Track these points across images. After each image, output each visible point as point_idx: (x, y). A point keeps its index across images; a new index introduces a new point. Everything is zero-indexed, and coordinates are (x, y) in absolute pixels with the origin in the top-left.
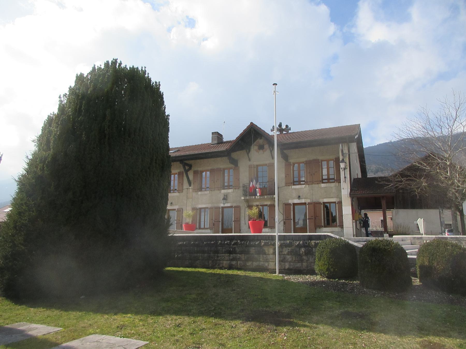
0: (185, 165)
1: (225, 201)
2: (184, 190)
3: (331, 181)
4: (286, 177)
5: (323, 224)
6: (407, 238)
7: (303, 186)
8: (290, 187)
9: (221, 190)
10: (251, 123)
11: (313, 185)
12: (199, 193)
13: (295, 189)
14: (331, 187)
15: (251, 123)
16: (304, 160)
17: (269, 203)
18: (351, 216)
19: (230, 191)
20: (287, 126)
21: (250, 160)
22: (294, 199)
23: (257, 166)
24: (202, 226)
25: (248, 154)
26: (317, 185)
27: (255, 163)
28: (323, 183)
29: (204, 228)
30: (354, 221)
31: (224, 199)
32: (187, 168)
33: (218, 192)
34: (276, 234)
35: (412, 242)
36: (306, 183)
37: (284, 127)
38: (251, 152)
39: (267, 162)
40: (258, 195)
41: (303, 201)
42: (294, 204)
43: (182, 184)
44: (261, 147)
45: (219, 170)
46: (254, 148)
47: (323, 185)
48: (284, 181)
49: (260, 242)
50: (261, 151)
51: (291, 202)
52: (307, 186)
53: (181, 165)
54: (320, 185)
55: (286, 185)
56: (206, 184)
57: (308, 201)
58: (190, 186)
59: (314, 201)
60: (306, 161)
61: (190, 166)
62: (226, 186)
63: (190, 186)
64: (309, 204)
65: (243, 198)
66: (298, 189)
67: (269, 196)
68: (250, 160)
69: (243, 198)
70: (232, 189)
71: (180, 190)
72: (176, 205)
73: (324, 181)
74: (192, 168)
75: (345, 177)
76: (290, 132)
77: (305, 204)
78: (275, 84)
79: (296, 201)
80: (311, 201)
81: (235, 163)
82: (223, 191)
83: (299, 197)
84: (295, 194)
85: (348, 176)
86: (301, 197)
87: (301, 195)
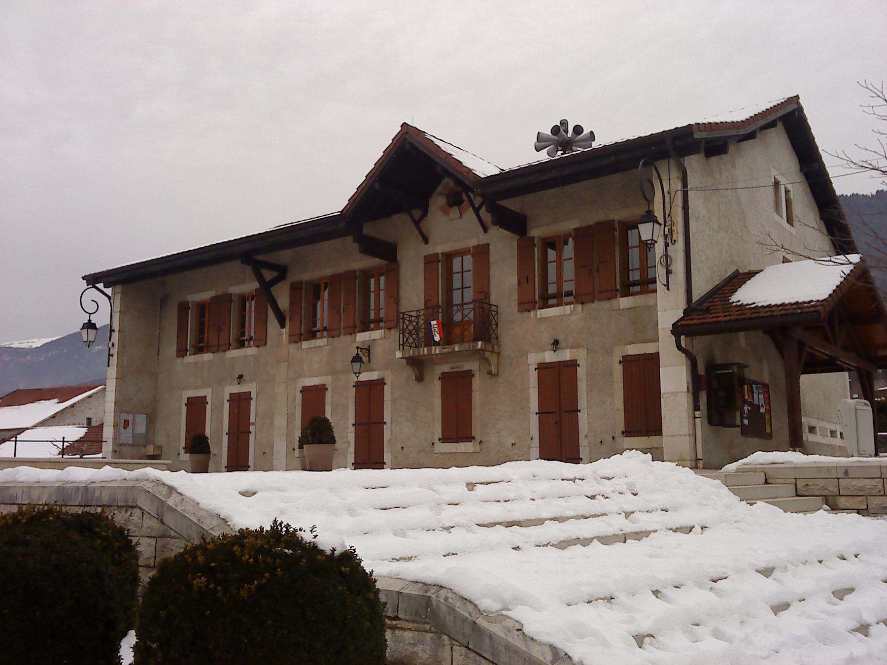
0: (257, 268)
1: (357, 366)
7: (568, 309)
8: (532, 313)
9: (355, 333)
11: (596, 305)
12: (305, 345)
13: (542, 319)
15: (404, 125)
16: (571, 225)
19: (377, 334)
21: (426, 241)
22: (543, 350)
23: (449, 257)
25: (417, 223)
26: (606, 304)
27: (440, 248)
30: (697, 413)
31: (357, 359)
32: (269, 275)
33: (348, 338)
36: (581, 297)
38: (430, 216)
39: (472, 243)
43: (265, 323)
44: (455, 201)
45: (350, 275)
47: (625, 302)
50: (455, 212)
52: (579, 307)
53: (248, 270)
60: (576, 230)
61: (282, 272)
65: (399, 354)
67: (466, 346)
68: (426, 241)
69: (399, 354)
72: (251, 381)
74: (288, 275)
81: (388, 253)
82: (362, 337)
83: (556, 343)
84: (546, 338)
85: (679, 267)
86: (562, 344)
87: (561, 338)
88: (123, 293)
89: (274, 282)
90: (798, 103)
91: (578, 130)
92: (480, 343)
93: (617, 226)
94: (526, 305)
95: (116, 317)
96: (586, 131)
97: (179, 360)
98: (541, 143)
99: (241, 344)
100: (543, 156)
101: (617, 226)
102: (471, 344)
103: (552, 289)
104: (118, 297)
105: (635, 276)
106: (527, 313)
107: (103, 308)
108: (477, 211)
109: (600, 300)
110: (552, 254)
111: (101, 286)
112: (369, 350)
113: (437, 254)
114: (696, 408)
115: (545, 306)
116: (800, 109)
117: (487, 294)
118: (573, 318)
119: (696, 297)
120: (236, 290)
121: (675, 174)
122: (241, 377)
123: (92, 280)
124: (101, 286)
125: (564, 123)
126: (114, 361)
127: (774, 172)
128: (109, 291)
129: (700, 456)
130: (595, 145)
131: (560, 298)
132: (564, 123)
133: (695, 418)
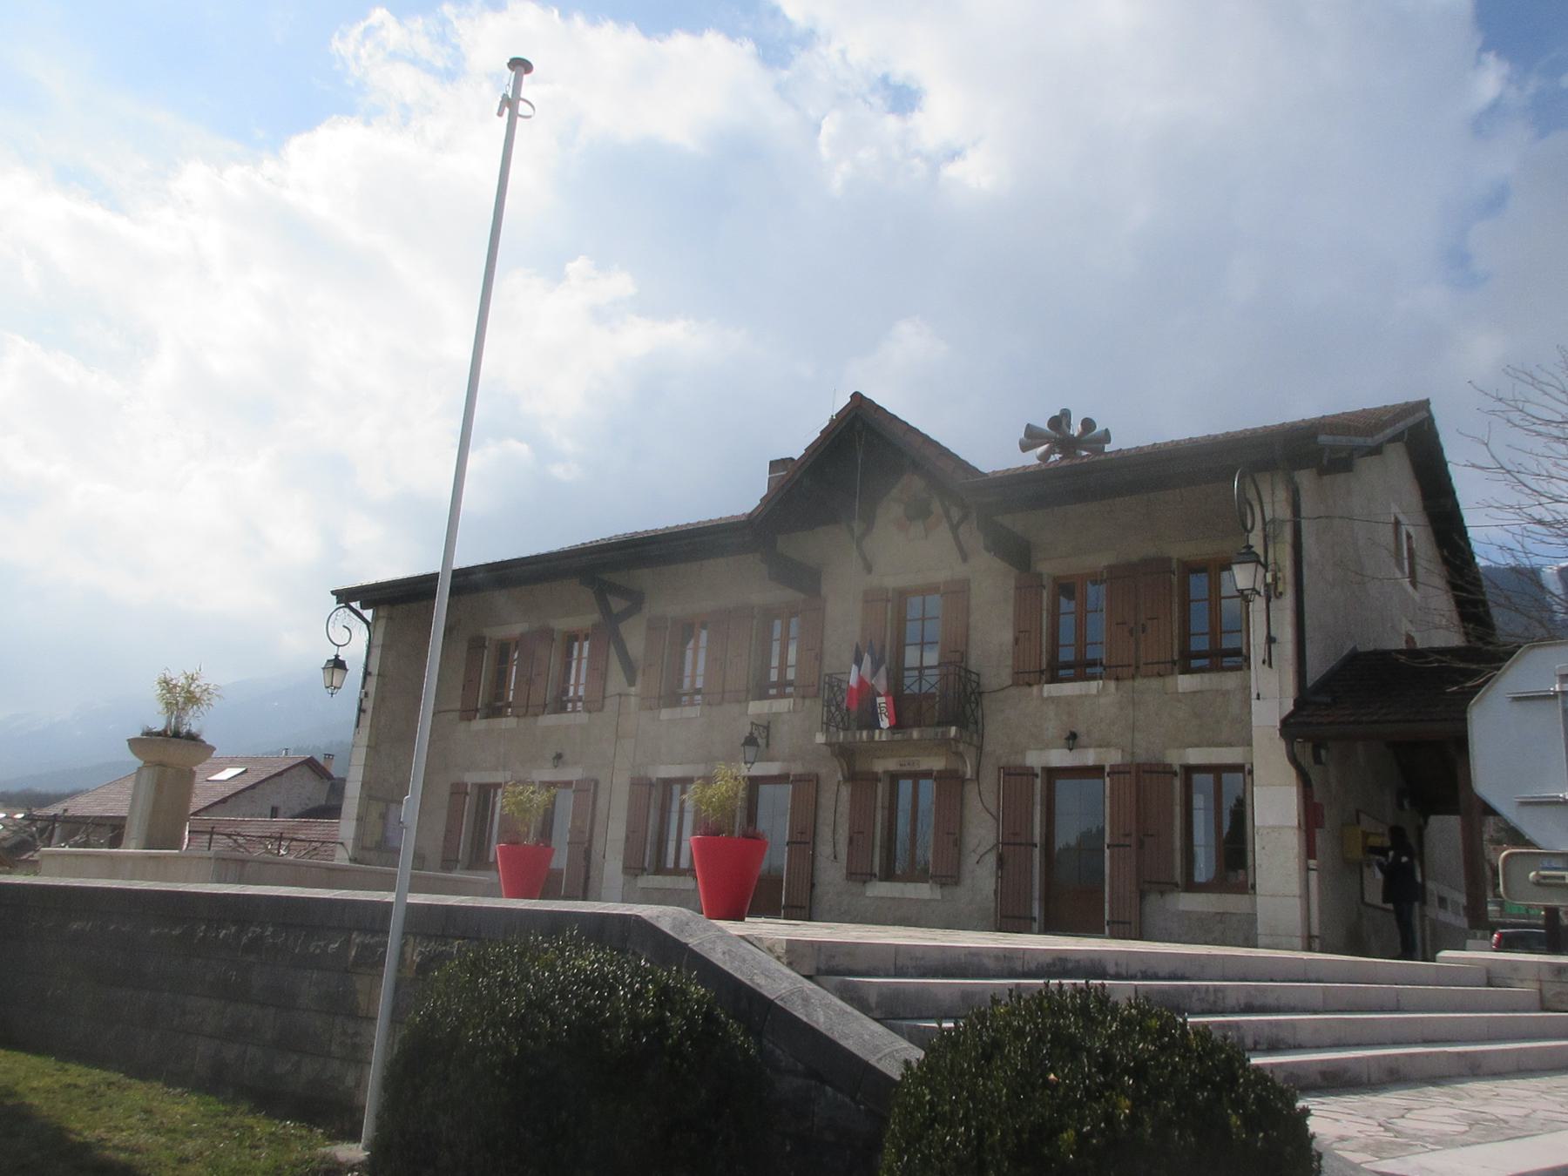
0: (603, 591)
1: (751, 751)
2: (607, 702)
3: (1227, 661)
4: (1017, 641)
5: (1178, 876)
6: (1515, 966)
7: (1093, 686)
8: (1035, 689)
9: (747, 701)
10: (857, 396)
11: (1140, 683)
12: (665, 714)
13: (1052, 699)
14: (1225, 693)
15: (857, 396)
17: (937, 763)
18: (1292, 841)
20: (1088, 424)
22: (1047, 746)
24: (670, 864)
26: (1155, 683)
27: (891, 582)
28: (1187, 670)
29: (677, 871)
30: (1312, 863)
31: (750, 741)
34: (390, 897)
35: (1548, 994)
37: (1076, 429)
39: (941, 576)
40: (885, 723)
41: (1089, 757)
42: (1052, 773)
44: (919, 512)
46: (891, 510)
47: (1185, 682)
48: (1010, 662)
49: (347, 943)
51: (1036, 759)
52: (1112, 685)
54: (1169, 680)
55: (1015, 684)
56: (694, 676)
57: (1112, 757)
58: (632, 683)
59: (1142, 757)
60: (1110, 568)
61: (636, 601)
62: (773, 685)
63: (632, 683)
64: (1116, 771)
65: (820, 738)
66: (1068, 701)
67: (930, 732)
68: (869, 569)
69: (820, 738)
70: (790, 696)
71: (595, 704)
73: (1195, 663)
75: (1270, 640)
76: (1108, 448)
77: (1096, 771)
78: (520, 66)
79: (1059, 757)
80: (1128, 759)
81: (805, 580)
82: (756, 708)
84: (1053, 727)
85: (1286, 634)
86: (1083, 739)
87: (1080, 729)
88: (390, 618)
89: (627, 614)
90: (1429, 411)
91: (1088, 424)
92: (953, 730)
93: (1174, 565)
94: (1025, 677)
95: (377, 652)
96: (1099, 428)
97: (463, 725)
98: (1032, 437)
99: (560, 707)
100: (1031, 458)
101: (1174, 565)
102: (940, 730)
103: (1067, 655)
104: (382, 623)
105: (1200, 643)
106: (1027, 690)
107: (354, 638)
108: (954, 529)
109: (1146, 676)
110: (1066, 605)
111: (356, 605)
112: (767, 728)
113: (1170, 559)
114: (1310, 851)
115: (1054, 679)
116: (1430, 420)
117: (964, 656)
118: (1102, 700)
119: (1309, 683)
120: (562, 624)
121: (1282, 495)
122: (559, 757)
123: (345, 597)
124: (356, 605)
125: (1066, 414)
126: (367, 720)
127: (1395, 509)
128: (368, 614)
129: (1315, 931)
130: (1108, 448)
131: (1082, 669)
132: (1066, 414)
133: (1308, 869)
